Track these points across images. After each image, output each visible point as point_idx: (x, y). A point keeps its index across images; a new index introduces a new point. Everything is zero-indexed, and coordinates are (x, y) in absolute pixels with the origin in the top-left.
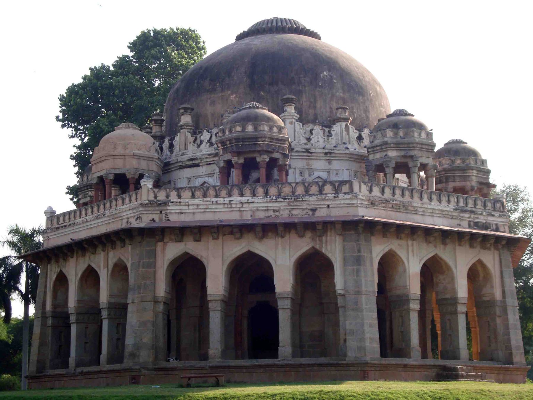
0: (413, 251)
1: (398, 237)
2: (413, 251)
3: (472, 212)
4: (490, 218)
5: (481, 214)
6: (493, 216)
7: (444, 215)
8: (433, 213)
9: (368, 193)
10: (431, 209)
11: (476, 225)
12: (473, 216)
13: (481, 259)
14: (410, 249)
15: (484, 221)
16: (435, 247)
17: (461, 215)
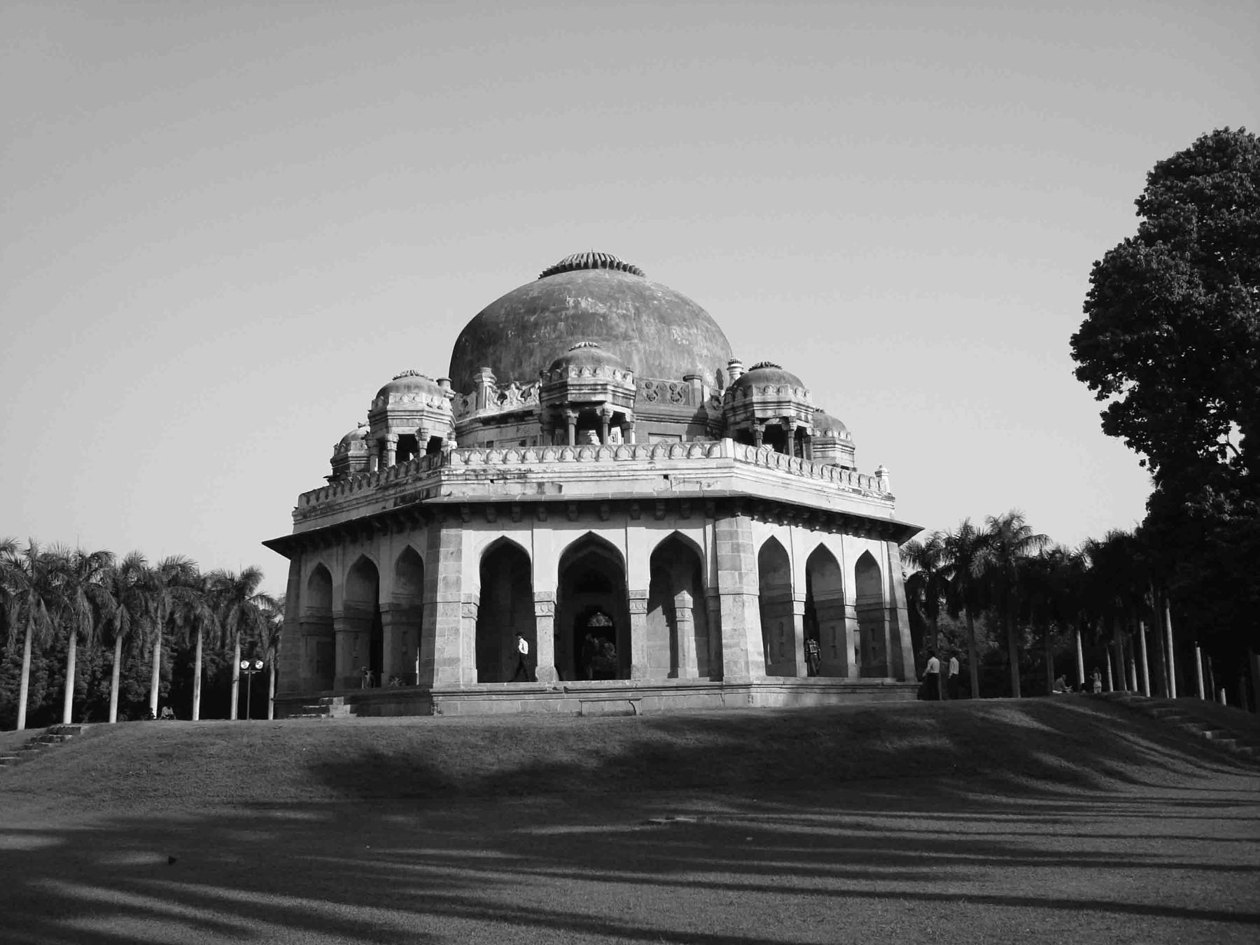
0: (337, 560)
1: (328, 545)
2: (337, 560)
3: (397, 485)
4: (419, 484)
5: (406, 484)
6: (420, 479)
7: (368, 501)
8: (358, 504)
9: (306, 504)
10: (354, 499)
11: (403, 499)
12: (399, 489)
13: (411, 545)
14: (335, 558)
15: (413, 491)
16: (362, 545)
17: (386, 494)
